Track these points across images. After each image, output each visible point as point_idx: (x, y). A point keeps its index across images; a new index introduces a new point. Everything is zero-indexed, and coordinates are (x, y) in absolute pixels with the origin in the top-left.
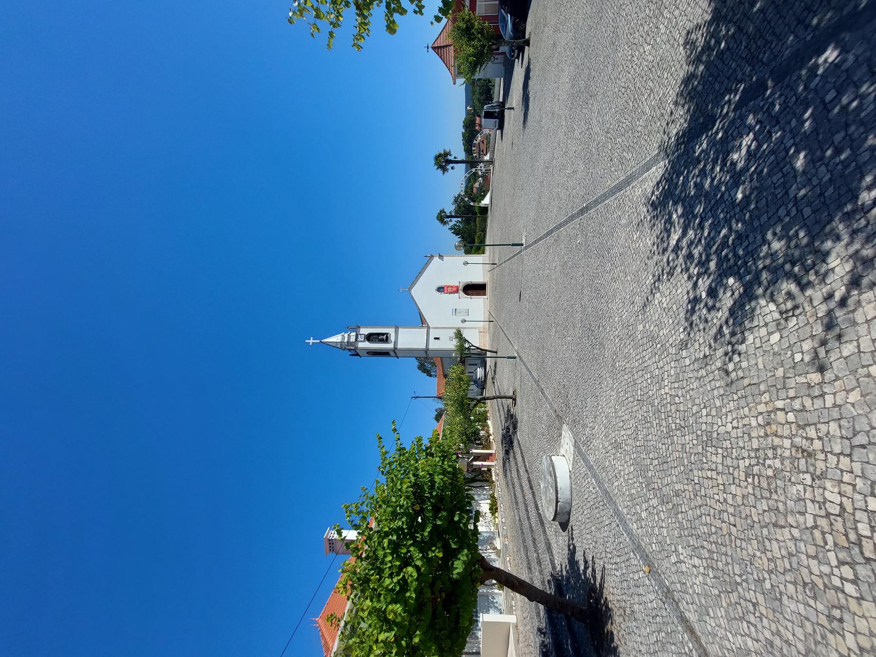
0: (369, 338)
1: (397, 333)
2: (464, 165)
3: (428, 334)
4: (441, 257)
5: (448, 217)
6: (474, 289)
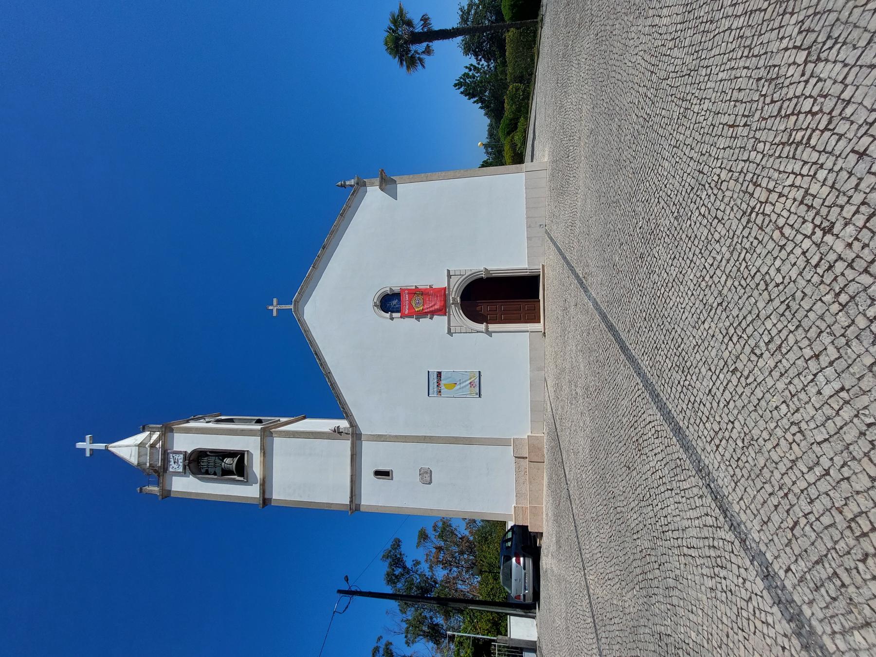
0: (200, 463)
1: (266, 452)
4: (387, 184)
5: (417, 38)
6: (502, 297)
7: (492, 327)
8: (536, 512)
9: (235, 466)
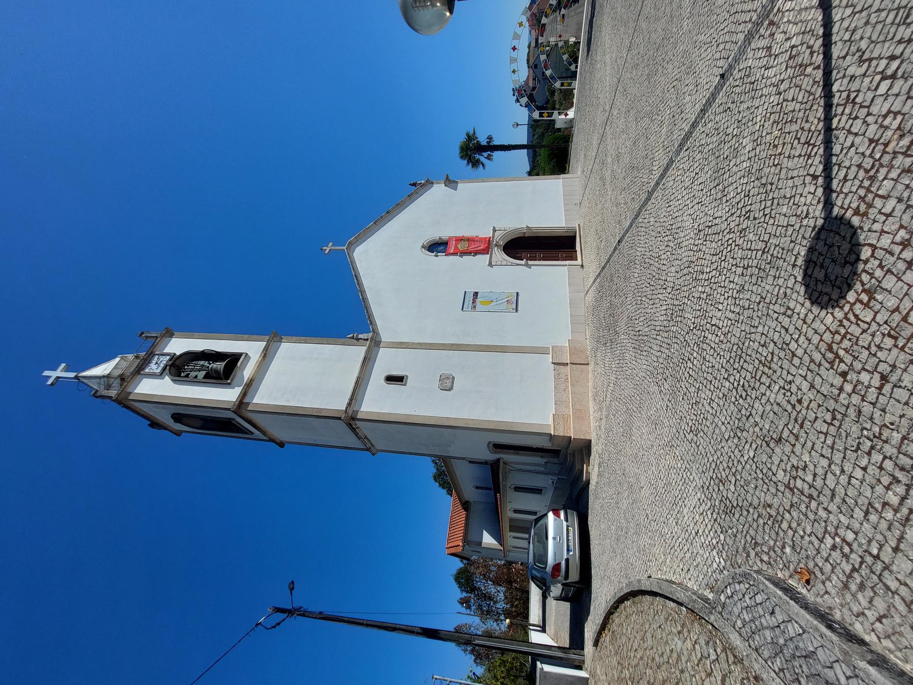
1: (267, 356)
2: (526, 150)
3: (368, 362)
5: (481, 149)
7: (530, 262)
8: (580, 415)
9: (224, 368)
